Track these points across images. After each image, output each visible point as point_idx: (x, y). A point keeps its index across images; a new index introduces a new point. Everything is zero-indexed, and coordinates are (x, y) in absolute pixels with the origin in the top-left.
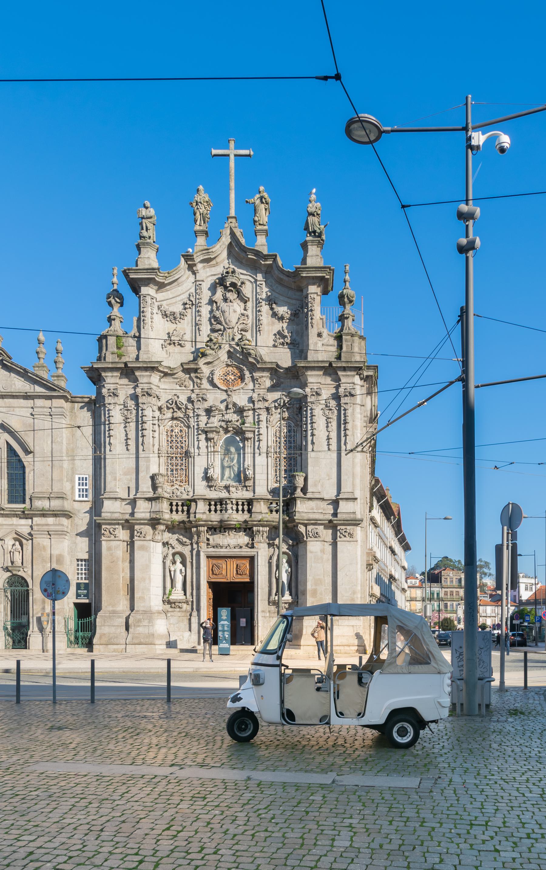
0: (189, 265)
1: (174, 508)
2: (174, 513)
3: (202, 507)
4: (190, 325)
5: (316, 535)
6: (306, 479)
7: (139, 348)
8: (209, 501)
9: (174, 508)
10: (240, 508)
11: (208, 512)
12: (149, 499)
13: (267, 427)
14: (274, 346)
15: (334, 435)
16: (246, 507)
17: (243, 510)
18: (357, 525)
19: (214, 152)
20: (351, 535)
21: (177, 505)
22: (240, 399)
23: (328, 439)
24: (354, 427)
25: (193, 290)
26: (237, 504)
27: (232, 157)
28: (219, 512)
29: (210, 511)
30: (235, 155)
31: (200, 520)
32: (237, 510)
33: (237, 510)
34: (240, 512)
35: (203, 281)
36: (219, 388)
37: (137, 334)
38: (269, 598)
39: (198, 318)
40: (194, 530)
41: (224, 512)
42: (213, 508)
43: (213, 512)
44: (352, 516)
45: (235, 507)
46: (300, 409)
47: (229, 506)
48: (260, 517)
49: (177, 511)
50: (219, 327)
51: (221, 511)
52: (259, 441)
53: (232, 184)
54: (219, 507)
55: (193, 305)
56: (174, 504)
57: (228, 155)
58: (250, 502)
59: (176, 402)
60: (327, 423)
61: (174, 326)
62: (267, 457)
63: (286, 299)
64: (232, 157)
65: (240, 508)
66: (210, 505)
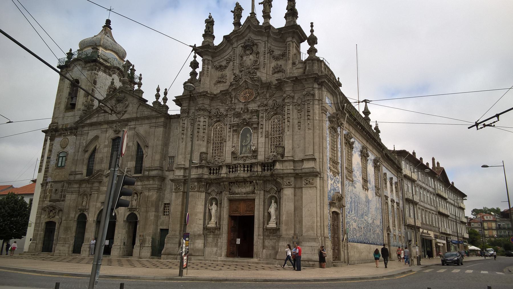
0: (228, 41)
5: (289, 184)
9: (212, 172)
10: (246, 169)
12: (197, 167)
16: (249, 169)
17: (248, 171)
18: (316, 176)
20: (312, 184)
21: (214, 170)
24: (314, 113)
25: (231, 53)
29: (230, 172)
31: (223, 178)
34: (246, 172)
38: (263, 227)
40: (222, 184)
44: (311, 170)
45: (242, 169)
49: (213, 173)
58: (252, 165)
63: (278, 48)
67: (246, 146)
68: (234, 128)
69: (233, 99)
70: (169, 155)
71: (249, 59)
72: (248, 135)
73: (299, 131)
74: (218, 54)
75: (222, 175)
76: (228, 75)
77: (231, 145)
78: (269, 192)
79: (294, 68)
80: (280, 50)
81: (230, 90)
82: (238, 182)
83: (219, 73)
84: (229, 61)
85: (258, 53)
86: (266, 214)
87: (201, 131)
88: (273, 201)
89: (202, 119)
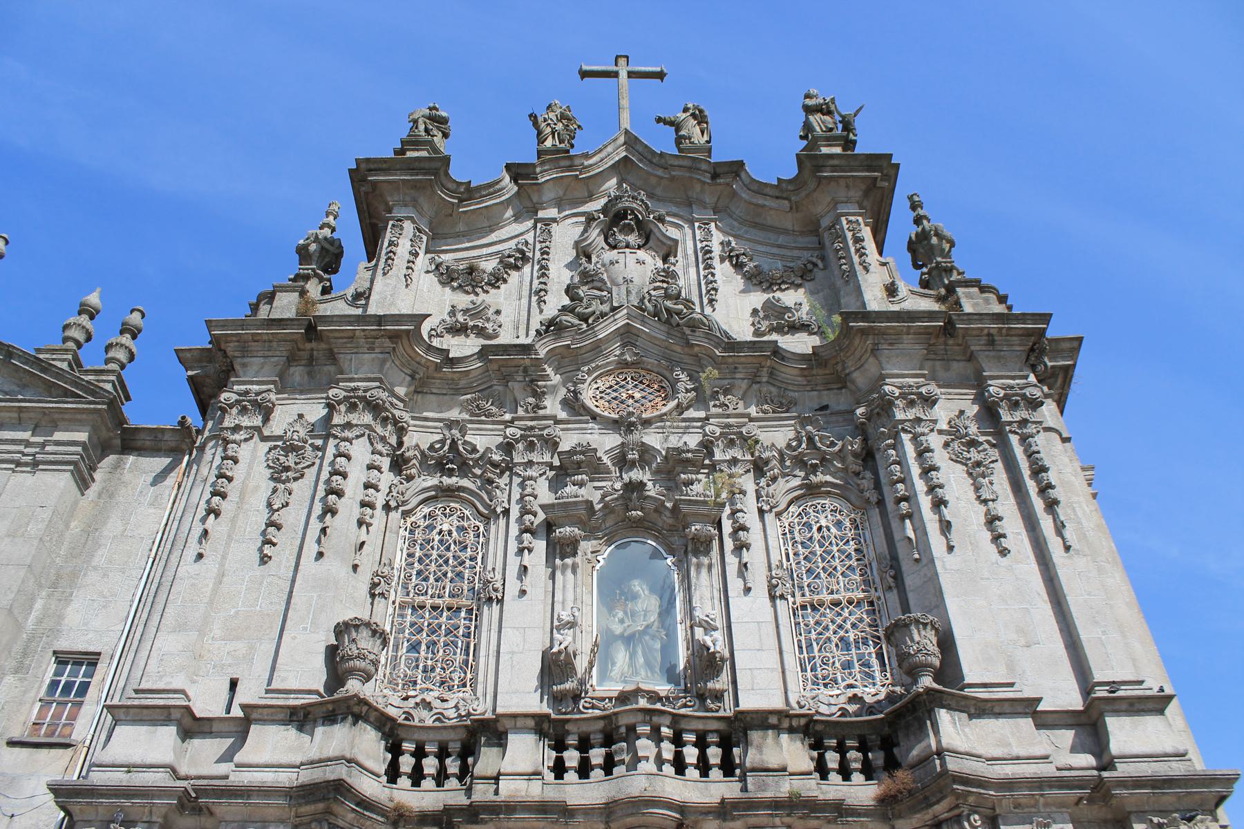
1: (406, 763)
2: (404, 782)
4: (515, 296)
6: (947, 643)
9: (406, 763)
10: (691, 754)
11: (550, 776)
12: (301, 718)
13: (761, 512)
15: (1007, 506)
19: (585, 68)
23: (992, 520)
25: (530, 237)
26: (678, 741)
27: (623, 75)
28: (597, 774)
29: (559, 769)
30: (631, 75)
32: (680, 766)
34: (692, 773)
35: (554, 220)
36: (594, 417)
39: (536, 282)
41: (619, 770)
42: (572, 758)
43: (571, 776)
45: (668, 750)
46: (868, 456)
47: (645, 746)
48: (784, 788)
49: (417, 776)
51: (609, 766)
52: (740, 547)
53: (625, 103)
55: (525, 258)
56: (408, 746)
57: (615, 75)
59: (454, 442)
60: (975, 480)
61: (472, 297)
62: (773, 598)
63: (775, 250)
64: (623, 75)
65: (691, 754)
66: (560, 746)
67: (629, 640)
68: (567, 531)
69: (548, 402)
70: (64, 644)
72: (637, 586)
73: (1004, 561)
74: (461, 227)
75: (508, 789)
77: (546, 619)
80: (782, 257)
81: (542, 353)
83: (463, 300)
85: (668, 252)
87: (348, 508)
89: (360, 451)
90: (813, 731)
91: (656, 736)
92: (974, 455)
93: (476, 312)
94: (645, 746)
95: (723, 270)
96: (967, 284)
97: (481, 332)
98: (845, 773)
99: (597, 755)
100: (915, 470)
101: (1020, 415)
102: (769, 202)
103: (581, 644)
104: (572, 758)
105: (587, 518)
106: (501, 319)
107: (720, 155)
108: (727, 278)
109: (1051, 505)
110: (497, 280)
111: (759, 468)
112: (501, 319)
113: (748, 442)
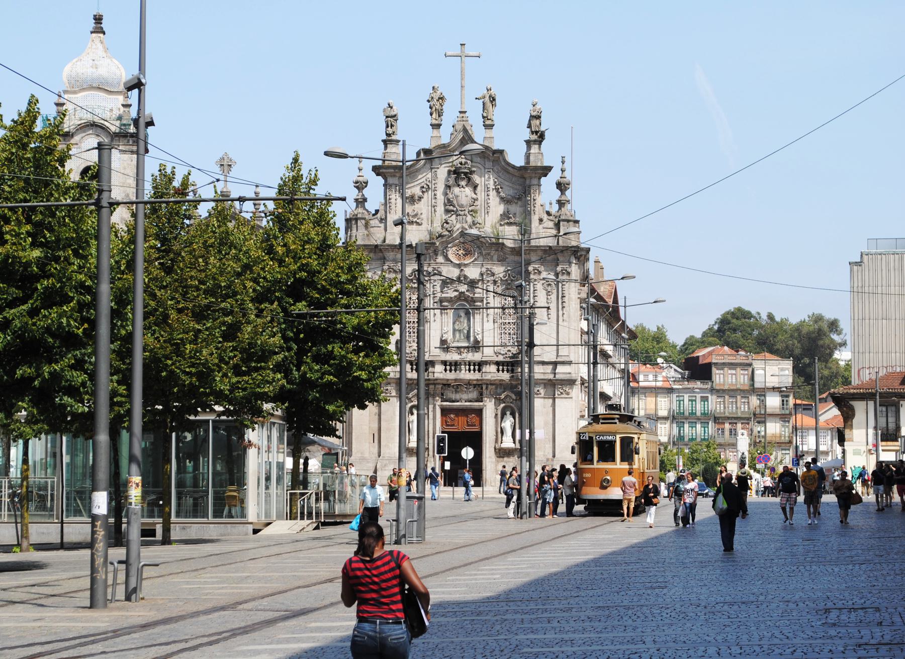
3: (439, 368)
7: (386, 230)
8: (444, 363)
10: (472, 367)
14: (501, 225)
16: (477, 367)
17: (474, 370)
22: (473, 273)
29: (446, 370)
32: (470, 370)
33: (470, 370)
37: (383, 217)
42: (448, 368)
48: (489, 377)
50: (451, 208)
51: (455, 370)
54: (453, 368)
65: (472, 367)
66: (446, 365)
71: (464, 194)
76: (424, 211)
78: (503, 401)
79: (541, 226)
82: (458, 386)
84: (425, 189)
85: (475, 187)
86: (499, 430)
88: (508, 413)
90: (497, 363)
91: (465, 365)
92: (549, 289)
93: (416, 215)
94: (463, 367)
95: (493, 194)
96: (564, 220)
97: (418, 224)
98: (503, 371)
99: (453, 368)
100: (532, 295)
101: (565, 277)
102: (510, 169)
103: (449, 337)
104: (448, 368)
105: (450, 300)
106: (422, 216)
107: (495, 147)
108: (494, 200)
109: (563, 307)
110: (420, 198)
111: (495, 282)
112: (422, 216)
113: (493, 275)
